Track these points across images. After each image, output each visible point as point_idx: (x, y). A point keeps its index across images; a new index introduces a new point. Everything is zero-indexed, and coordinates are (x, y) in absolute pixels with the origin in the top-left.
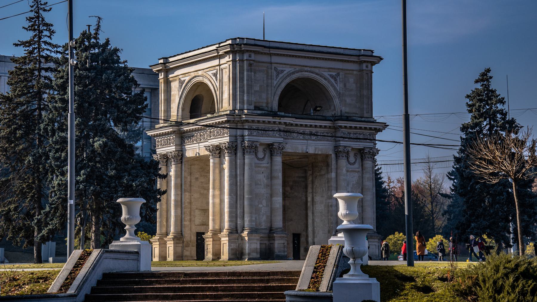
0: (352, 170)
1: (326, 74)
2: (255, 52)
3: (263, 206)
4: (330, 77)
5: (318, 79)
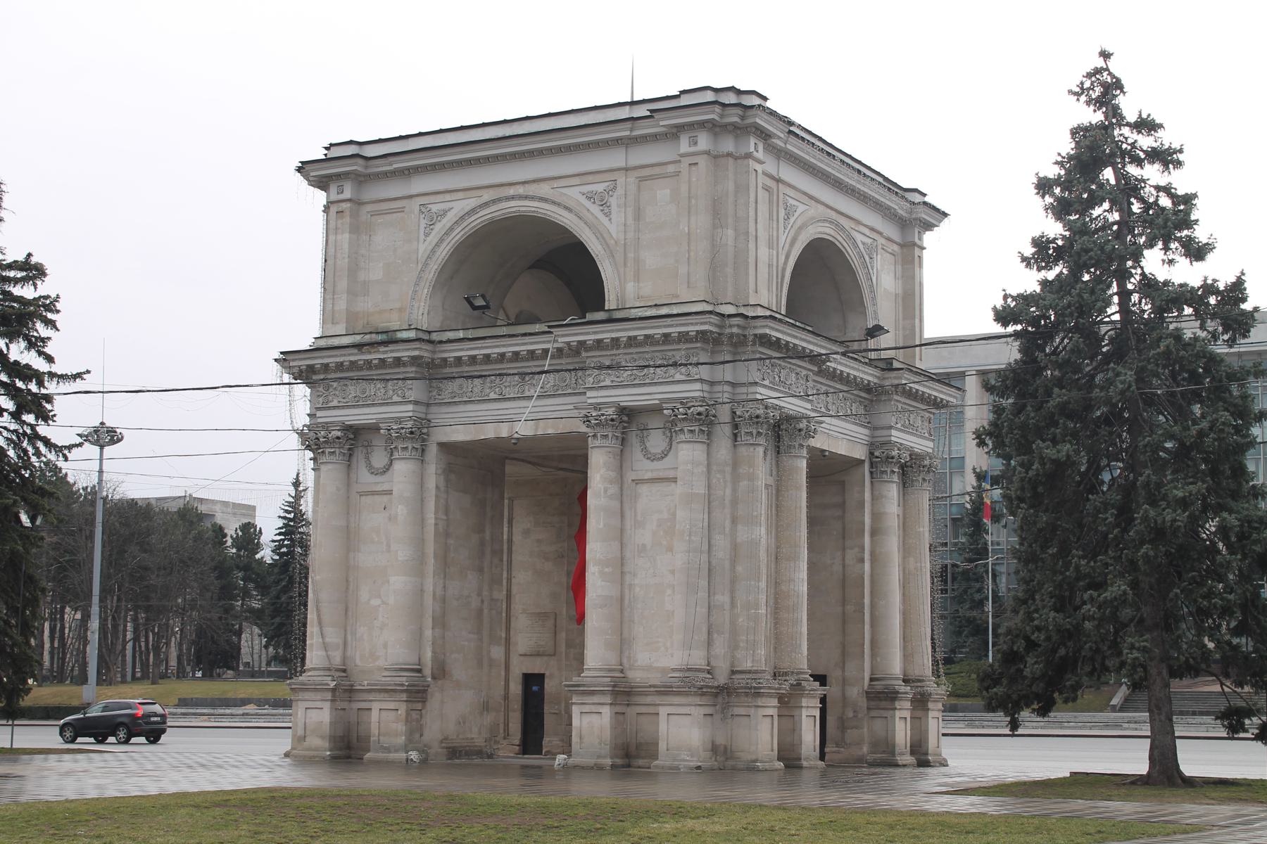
0: (655, 475)
1: (574, 194)
2: (361, 180)
3: (384, 603)
4: (589, 198)
5: (549, 213)
